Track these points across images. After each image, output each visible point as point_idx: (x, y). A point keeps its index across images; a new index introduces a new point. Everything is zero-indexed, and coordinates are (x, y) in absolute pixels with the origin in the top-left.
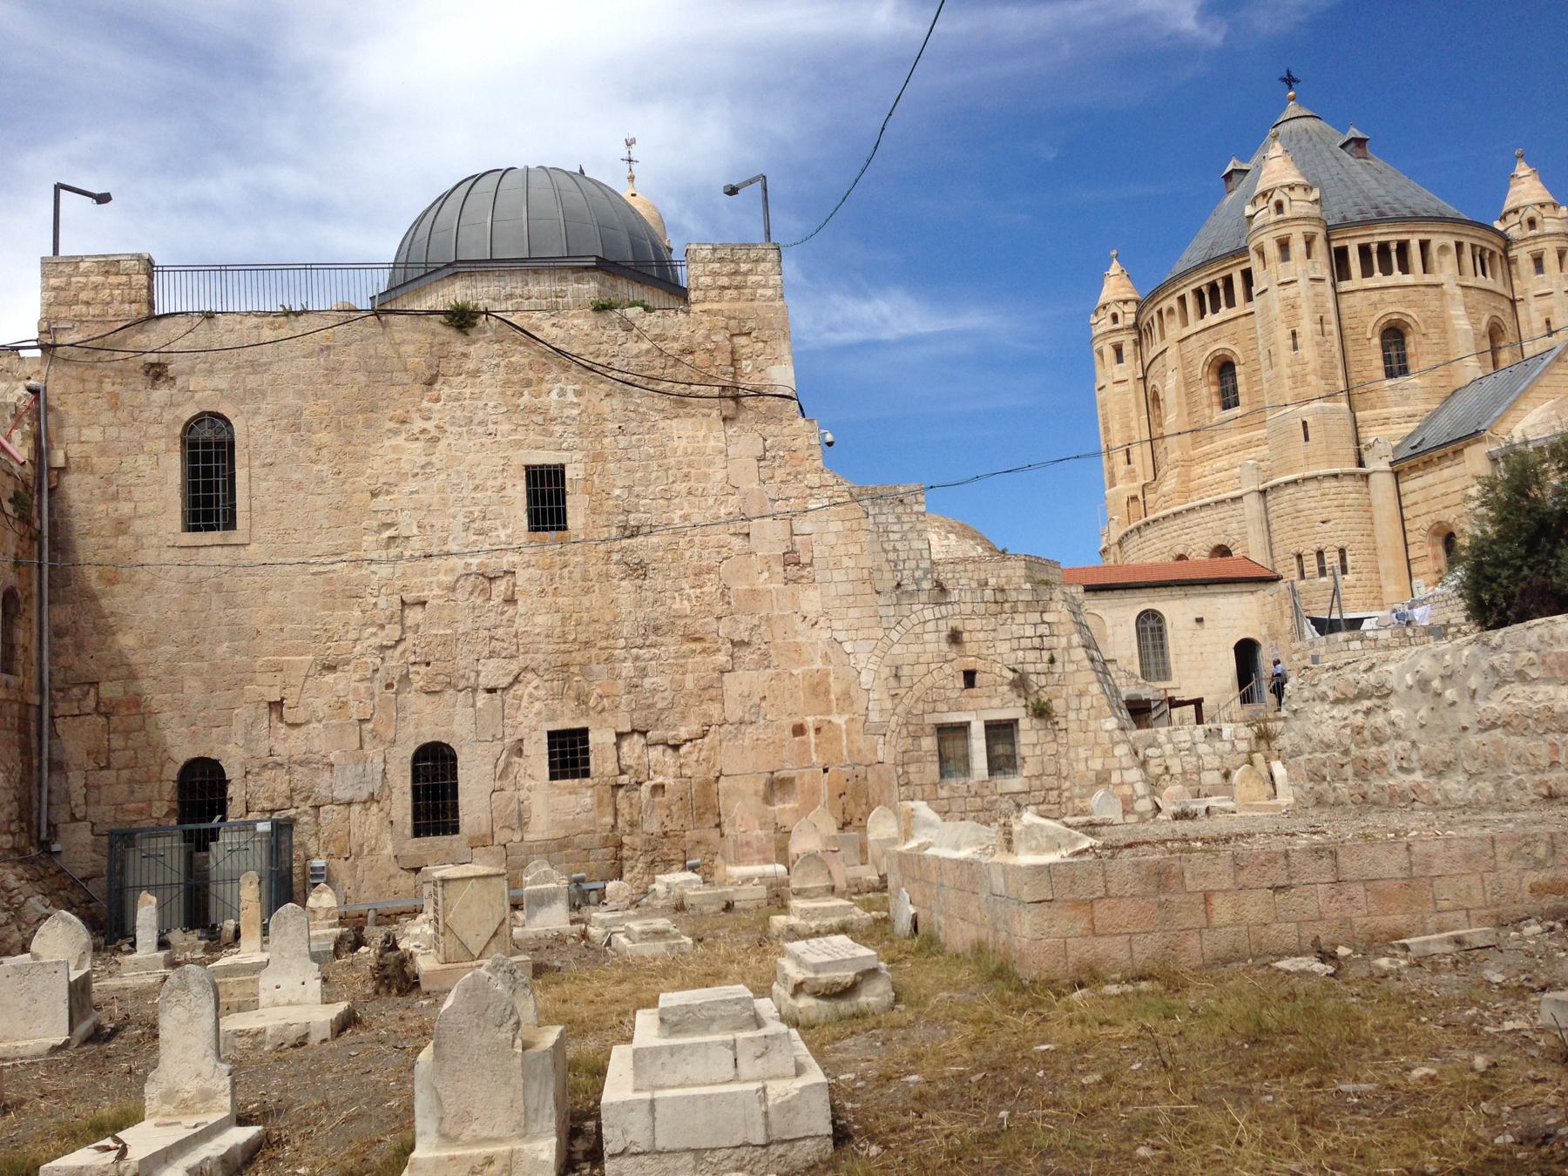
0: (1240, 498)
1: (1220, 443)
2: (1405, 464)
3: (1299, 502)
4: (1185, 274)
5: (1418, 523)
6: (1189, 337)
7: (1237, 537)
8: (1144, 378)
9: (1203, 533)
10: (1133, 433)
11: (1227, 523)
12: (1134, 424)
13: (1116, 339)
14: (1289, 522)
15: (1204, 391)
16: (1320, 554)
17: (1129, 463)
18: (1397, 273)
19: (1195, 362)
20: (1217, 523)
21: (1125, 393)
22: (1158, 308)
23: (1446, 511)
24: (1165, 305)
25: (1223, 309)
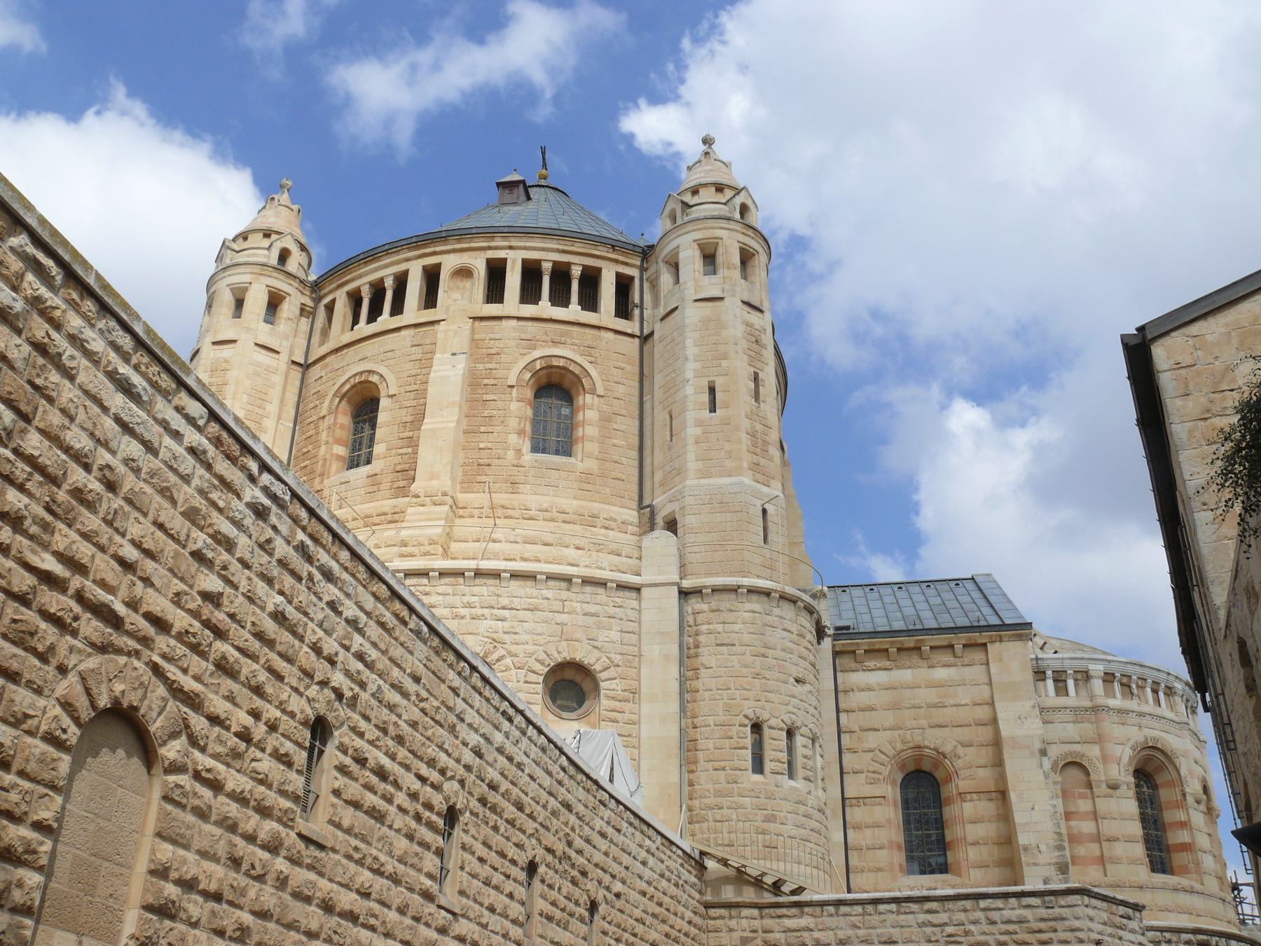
0: (638, 589)
2: (864, 643)
3: (769, 631)
4: (527, 232)
5: (872, 740)
7: (617, 659)
8: (305, 367)
9: (540, 628)
11: (600, 627)
13: (281, 284)
14: (748, 659)
15: (514, 406)
16: (790, 733)
19: (503, 358)
20: (580, 620)
21: (270, 370)
23: (936, 731)
24: (449, 263)
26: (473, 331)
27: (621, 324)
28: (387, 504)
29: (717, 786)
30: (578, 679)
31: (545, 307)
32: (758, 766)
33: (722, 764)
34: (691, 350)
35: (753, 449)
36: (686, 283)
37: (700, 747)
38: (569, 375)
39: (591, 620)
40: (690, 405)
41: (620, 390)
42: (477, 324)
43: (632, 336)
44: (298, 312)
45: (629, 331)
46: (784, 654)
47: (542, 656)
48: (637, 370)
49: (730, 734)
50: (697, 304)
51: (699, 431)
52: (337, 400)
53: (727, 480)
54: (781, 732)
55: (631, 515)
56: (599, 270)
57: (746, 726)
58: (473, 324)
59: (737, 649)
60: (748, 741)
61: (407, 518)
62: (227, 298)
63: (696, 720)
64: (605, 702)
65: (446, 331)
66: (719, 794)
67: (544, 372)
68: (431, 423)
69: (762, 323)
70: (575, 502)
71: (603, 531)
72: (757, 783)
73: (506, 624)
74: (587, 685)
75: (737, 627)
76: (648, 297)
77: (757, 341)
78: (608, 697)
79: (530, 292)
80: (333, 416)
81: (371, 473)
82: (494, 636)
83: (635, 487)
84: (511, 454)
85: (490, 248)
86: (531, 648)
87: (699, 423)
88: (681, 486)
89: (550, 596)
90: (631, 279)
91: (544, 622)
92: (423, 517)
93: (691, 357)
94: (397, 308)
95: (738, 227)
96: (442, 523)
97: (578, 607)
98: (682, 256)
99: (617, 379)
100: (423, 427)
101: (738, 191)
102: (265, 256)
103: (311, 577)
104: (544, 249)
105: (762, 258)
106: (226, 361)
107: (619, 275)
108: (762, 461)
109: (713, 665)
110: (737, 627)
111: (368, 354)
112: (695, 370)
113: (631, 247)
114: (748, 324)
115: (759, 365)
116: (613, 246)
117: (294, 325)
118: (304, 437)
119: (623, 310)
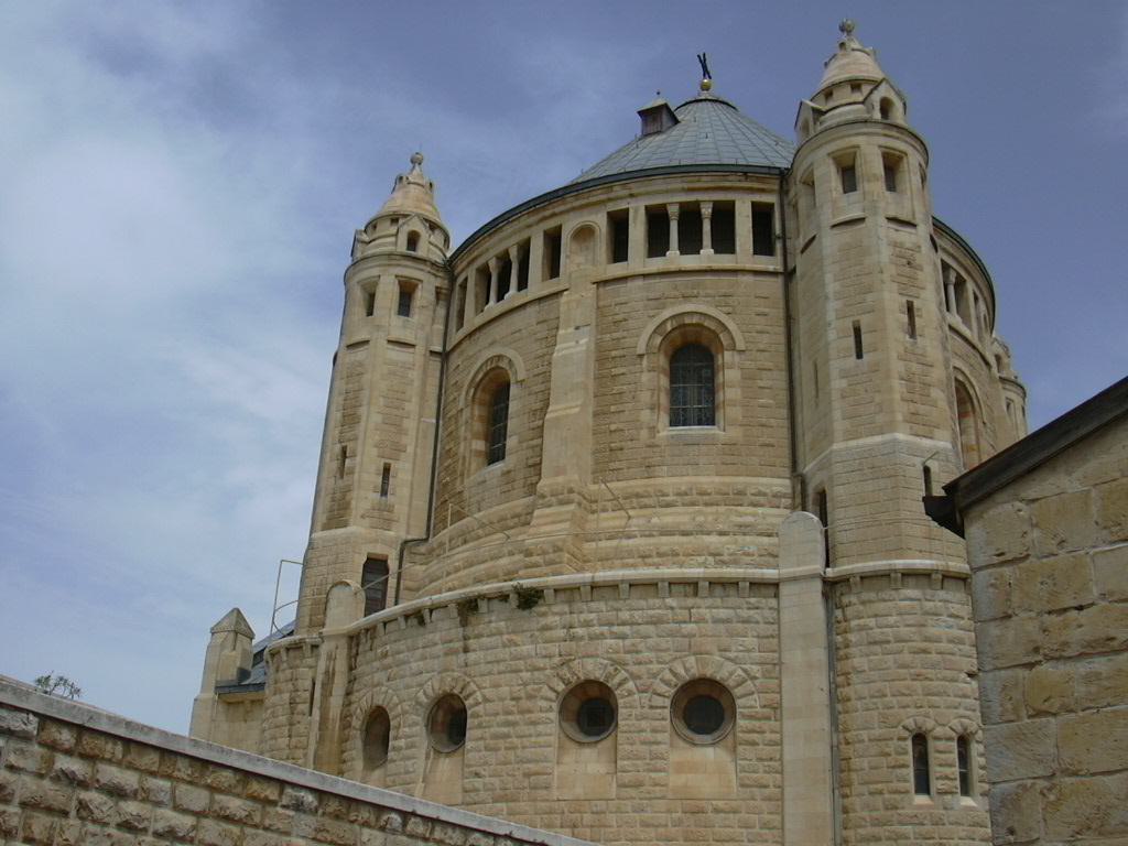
0: (774, 586)
1: (668, 482)
3: (930, 620)
6: (624, 279)
7: (755, 669)
8: (444, 356)
9: (665, 643)
10: (405, 440)
12: (410, 424)
13: (411, 271)
15: (645, 377)
16: (963, 741)
17: (384, 492)
18: (958, 319)
20: (709, 627)
22: (551, 224)
27: (764, 263)
28: (520, 503)
29: (875, 814)
30: (714, 695)
31: (674, 258)
32: (923, 785)
33: (879, 786)
34: (832, 287)
35: (908, 396)
36: (822, 206)
37: (853, 767)
38: (706, 332)
39: (721, 627)
40: (833, 352)
41: (765, 339)
42: (601, 289)
43: (774, 274)
44: (432, 297)
45: (771, 268)
46: (951, 645)
47: (668, 676)
48: (781, 313)
49: (887, 750)
50: (835, 231)
51: (844, 383)
52: (472, 391)
53: (878, 439)
54: (950, 743)
55: (782, 484)
56: (733, 202)
57: (905, 739)
58: (598, 288)
59: (894, 646)
60: (909, 758)
61: (533, 522)
62: (358, 294)
63: (848, 735)
64: (741, 722)
65: (568, 303)
66: (877, 823)
67: (676, 333)
68: (556, 411)
69: (914, 238)
70: (717, 479)
71: (751, 510)
72: (920, 807)
73: (628, 642)
74: (724, 702)
75: (892, 620)
76: (790, 225)
77: (909, 263)
78: (744, 717)
79: (657, 245)
80: (469, 408)
81: (505, 469)
82: (614, 656)
83: (786, 451)
84: (644, 434)
85: (610, 200)
86: (655, 667)
87: (845, 374)
88: (827, 452)
89: (674, 604)
90: (771, 206)
91: (668, 636)
92: (550, 519)
93: (831, 296)
94: (523, 284)
96: (566, 525)
97: (707, 613)
98: (817, 174)
99: (759, 328)
100: (548, 416)
101: (876, 84)
102: (390, 244)
103: (82, 805)
104: (667, 191)
105: (913, 159)
106: (361, 364)
107: (754, 205)
108: (922, 409)
109: (866, 668)
110: (892, 620)
111: (498, 337)
112: (837, 310)
113: (766, 170)
114: (895, 245)
115: (913, 291)
116: (745, 173)
117: (431, 313)
118: (446, 433)
119: (763, 244)
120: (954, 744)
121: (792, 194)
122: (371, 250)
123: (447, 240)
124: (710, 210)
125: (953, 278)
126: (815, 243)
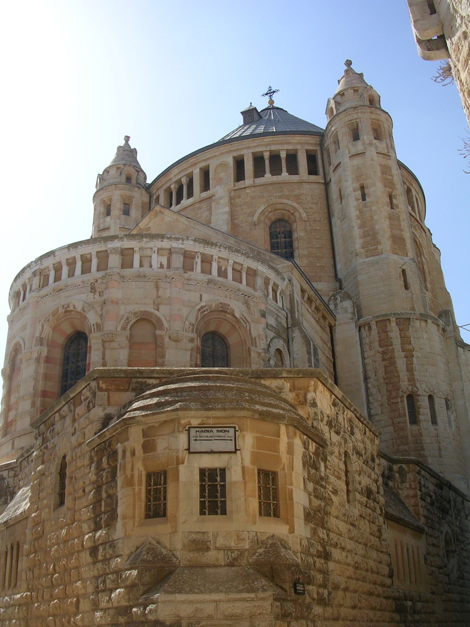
16: (431, 398)
22: (203, 164)
25: (285, 175)
26: (231, 198)
27: (313, 178)
56: (296, 150)
79: (259, 171)
90: (317, 150)
94: (190, 194)
95: (369, 110)
107: (307, 151)
119: (313, 171)
120: (427, 399)
121: (326, 145)
122: (105, 183)
123: (145, 178)
124: (285, 155)
125: (406, 187)
126: (341, 165)
